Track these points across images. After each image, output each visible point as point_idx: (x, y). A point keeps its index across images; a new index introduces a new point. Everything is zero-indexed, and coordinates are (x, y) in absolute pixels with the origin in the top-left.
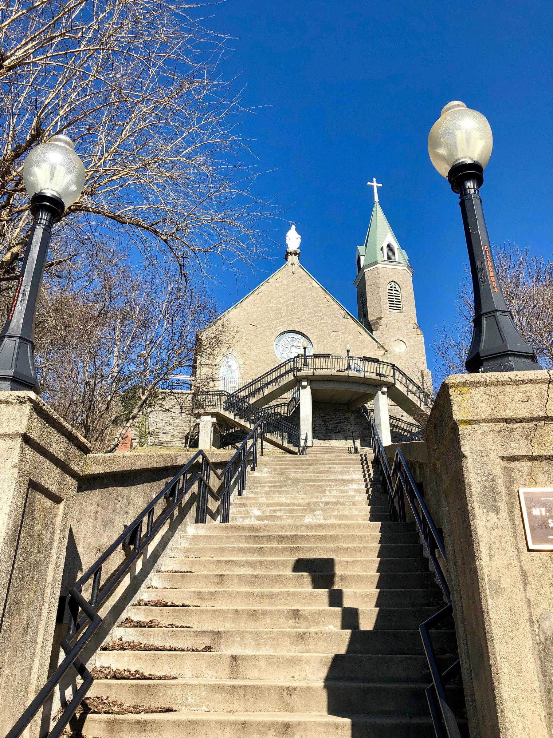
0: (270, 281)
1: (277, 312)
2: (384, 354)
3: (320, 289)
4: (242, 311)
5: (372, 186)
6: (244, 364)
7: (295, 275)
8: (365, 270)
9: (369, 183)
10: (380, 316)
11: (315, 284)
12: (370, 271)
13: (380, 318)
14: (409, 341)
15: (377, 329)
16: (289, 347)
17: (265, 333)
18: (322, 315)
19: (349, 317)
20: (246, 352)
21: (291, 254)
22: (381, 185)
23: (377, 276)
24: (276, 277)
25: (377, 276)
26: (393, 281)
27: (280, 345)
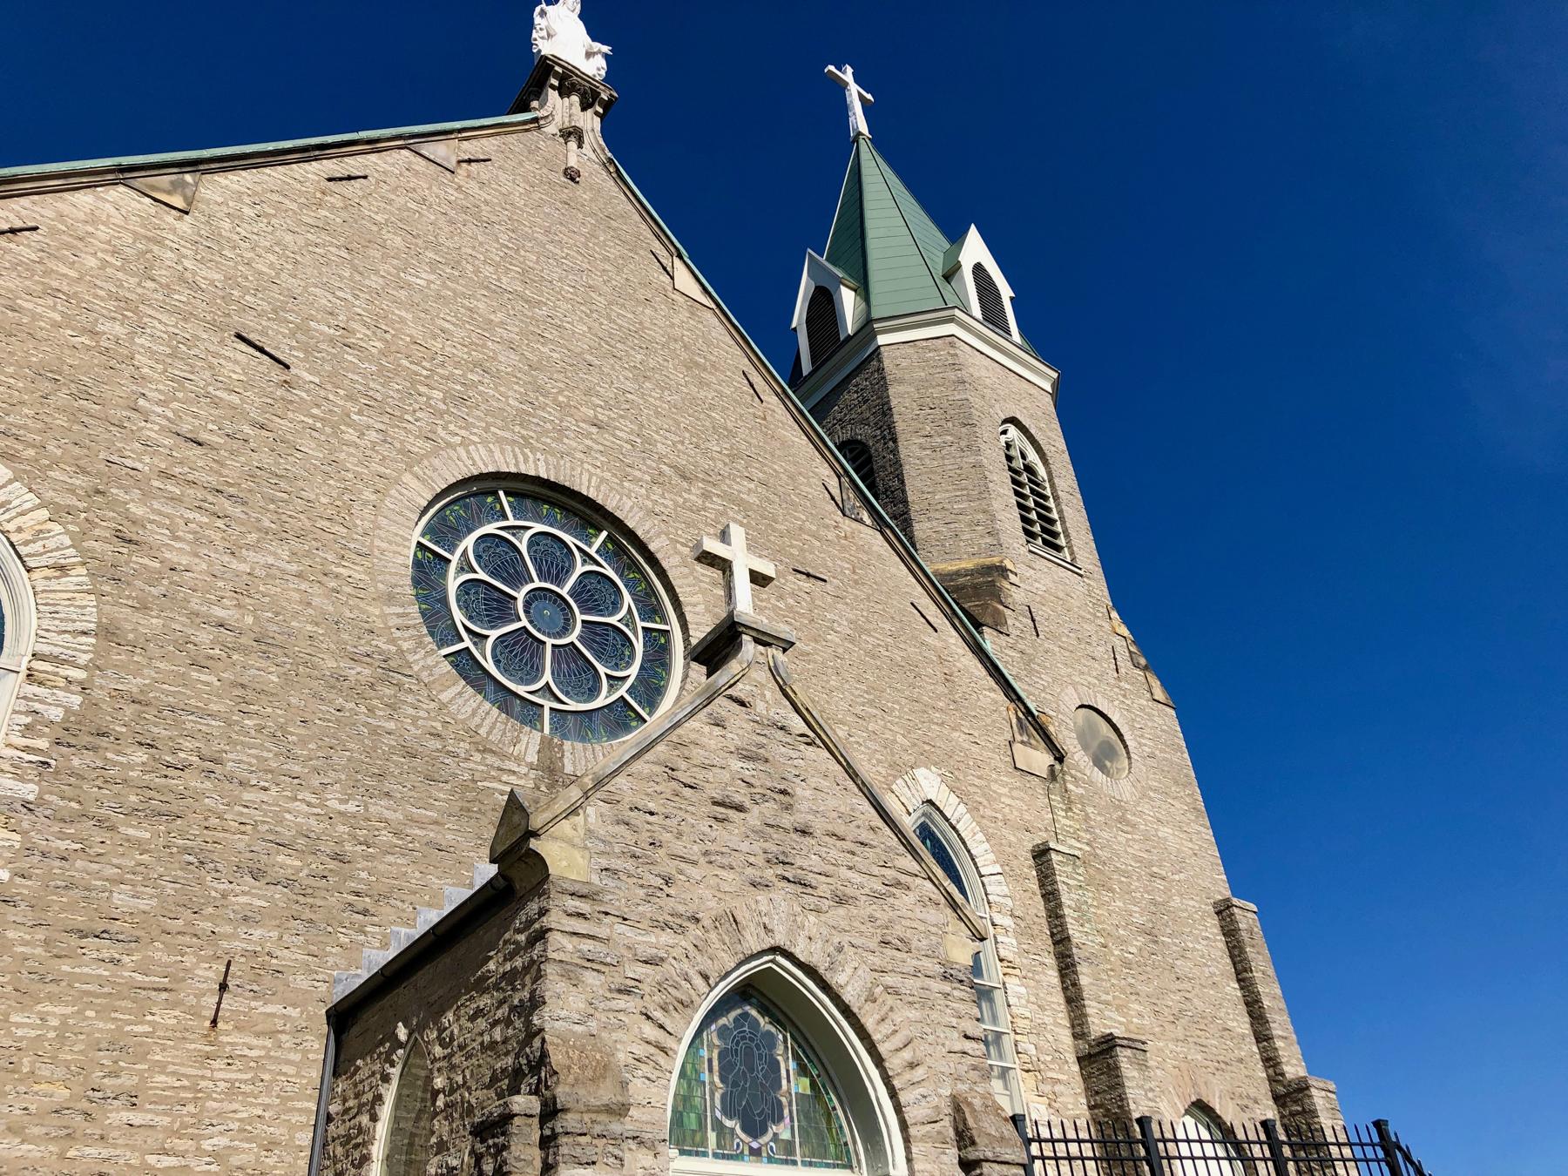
0: (428, 149)
1: (460, 334)
2: (1053, 775)
3: (711, 319)
4: (185, 225)
5: (843, 86)
6: (107, 633)
7: (582, 193)
8: (882, 340)
9: (832, 68)
10: (996, 560)
11: (684, 279)
12: (908, 350)
13: (1003, 571)
14: (1132, 728)
15: (999, 626)
16: (520, 595)
17: (350, 434)
18: (733, 457)
19: (865, 516)
20: (160, 535)
21: (564, 92)
22: (869, 96)
23: (952, 376)
24: (471, 148)
25: (952, 376)
26: (1013, 421)
27: (455, 559)
